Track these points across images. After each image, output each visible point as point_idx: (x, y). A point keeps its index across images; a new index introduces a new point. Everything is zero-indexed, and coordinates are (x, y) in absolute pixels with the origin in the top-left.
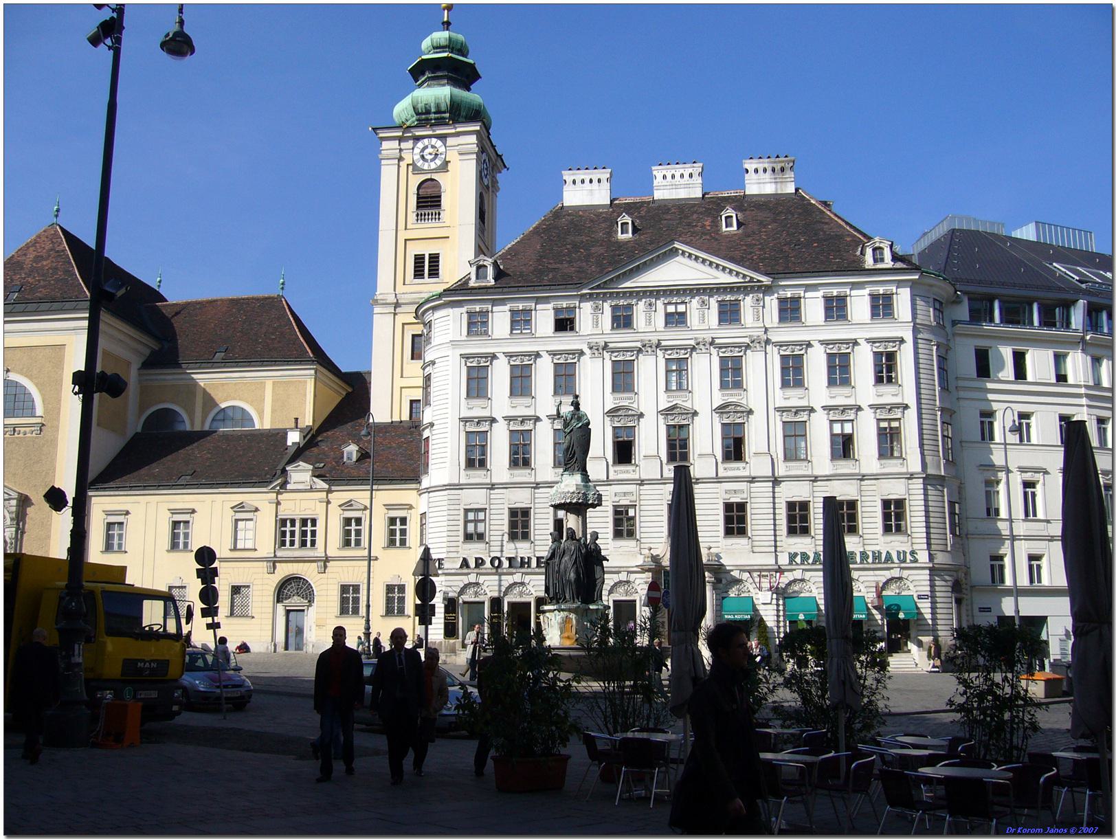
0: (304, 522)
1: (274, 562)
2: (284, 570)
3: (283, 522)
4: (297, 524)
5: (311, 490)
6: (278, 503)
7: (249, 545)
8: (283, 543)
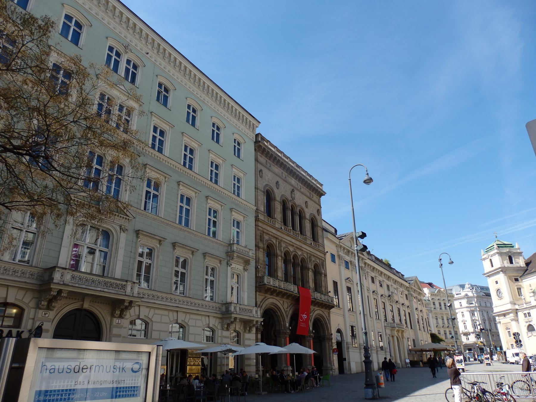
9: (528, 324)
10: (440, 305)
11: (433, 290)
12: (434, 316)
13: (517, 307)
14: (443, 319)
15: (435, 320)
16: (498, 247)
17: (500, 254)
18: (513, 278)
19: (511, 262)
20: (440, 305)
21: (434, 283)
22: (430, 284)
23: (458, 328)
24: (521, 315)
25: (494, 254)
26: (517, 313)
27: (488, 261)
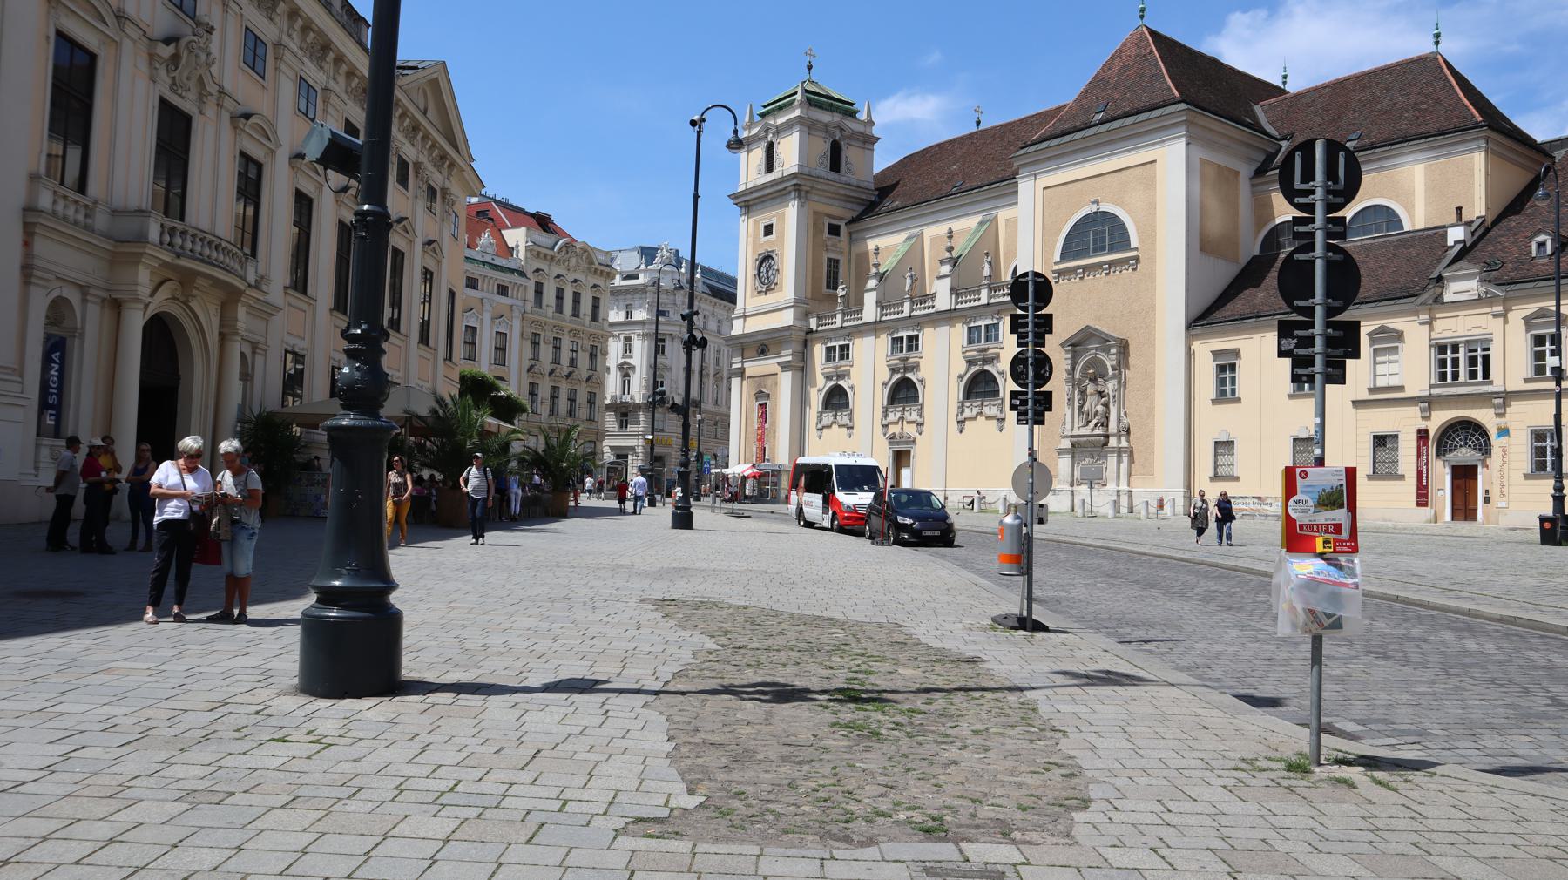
0: (1471, 346)
1: (1429, 403)
2: (1440, 418)
3: (1442, 349)
4: (1462, 350)
5: (1479, 302)
6: (1430, 323)
7: (1395, 381)
8: (1443, 377)
9: (831, 384)
10: (560, 296)
11: (544, 239)
12: (529, 331)
13: (813, 323)
14: (557, 348)
15: (528, 344)
16: (809, 100)
17: (808, 126)
18: (827, 221)
19: (835, 165)
20: (560, 296)
21: (558, 221)
22: (543, 222)
23: (601, 384)
24: (819, 351)
25: (788, 126)
26: (805, 343)
27: (758, 154)
